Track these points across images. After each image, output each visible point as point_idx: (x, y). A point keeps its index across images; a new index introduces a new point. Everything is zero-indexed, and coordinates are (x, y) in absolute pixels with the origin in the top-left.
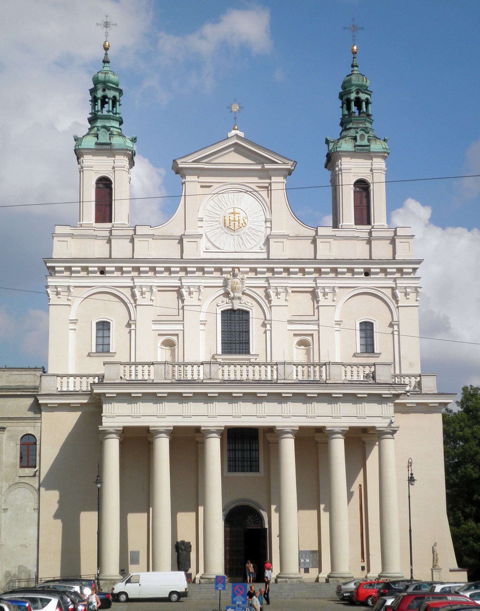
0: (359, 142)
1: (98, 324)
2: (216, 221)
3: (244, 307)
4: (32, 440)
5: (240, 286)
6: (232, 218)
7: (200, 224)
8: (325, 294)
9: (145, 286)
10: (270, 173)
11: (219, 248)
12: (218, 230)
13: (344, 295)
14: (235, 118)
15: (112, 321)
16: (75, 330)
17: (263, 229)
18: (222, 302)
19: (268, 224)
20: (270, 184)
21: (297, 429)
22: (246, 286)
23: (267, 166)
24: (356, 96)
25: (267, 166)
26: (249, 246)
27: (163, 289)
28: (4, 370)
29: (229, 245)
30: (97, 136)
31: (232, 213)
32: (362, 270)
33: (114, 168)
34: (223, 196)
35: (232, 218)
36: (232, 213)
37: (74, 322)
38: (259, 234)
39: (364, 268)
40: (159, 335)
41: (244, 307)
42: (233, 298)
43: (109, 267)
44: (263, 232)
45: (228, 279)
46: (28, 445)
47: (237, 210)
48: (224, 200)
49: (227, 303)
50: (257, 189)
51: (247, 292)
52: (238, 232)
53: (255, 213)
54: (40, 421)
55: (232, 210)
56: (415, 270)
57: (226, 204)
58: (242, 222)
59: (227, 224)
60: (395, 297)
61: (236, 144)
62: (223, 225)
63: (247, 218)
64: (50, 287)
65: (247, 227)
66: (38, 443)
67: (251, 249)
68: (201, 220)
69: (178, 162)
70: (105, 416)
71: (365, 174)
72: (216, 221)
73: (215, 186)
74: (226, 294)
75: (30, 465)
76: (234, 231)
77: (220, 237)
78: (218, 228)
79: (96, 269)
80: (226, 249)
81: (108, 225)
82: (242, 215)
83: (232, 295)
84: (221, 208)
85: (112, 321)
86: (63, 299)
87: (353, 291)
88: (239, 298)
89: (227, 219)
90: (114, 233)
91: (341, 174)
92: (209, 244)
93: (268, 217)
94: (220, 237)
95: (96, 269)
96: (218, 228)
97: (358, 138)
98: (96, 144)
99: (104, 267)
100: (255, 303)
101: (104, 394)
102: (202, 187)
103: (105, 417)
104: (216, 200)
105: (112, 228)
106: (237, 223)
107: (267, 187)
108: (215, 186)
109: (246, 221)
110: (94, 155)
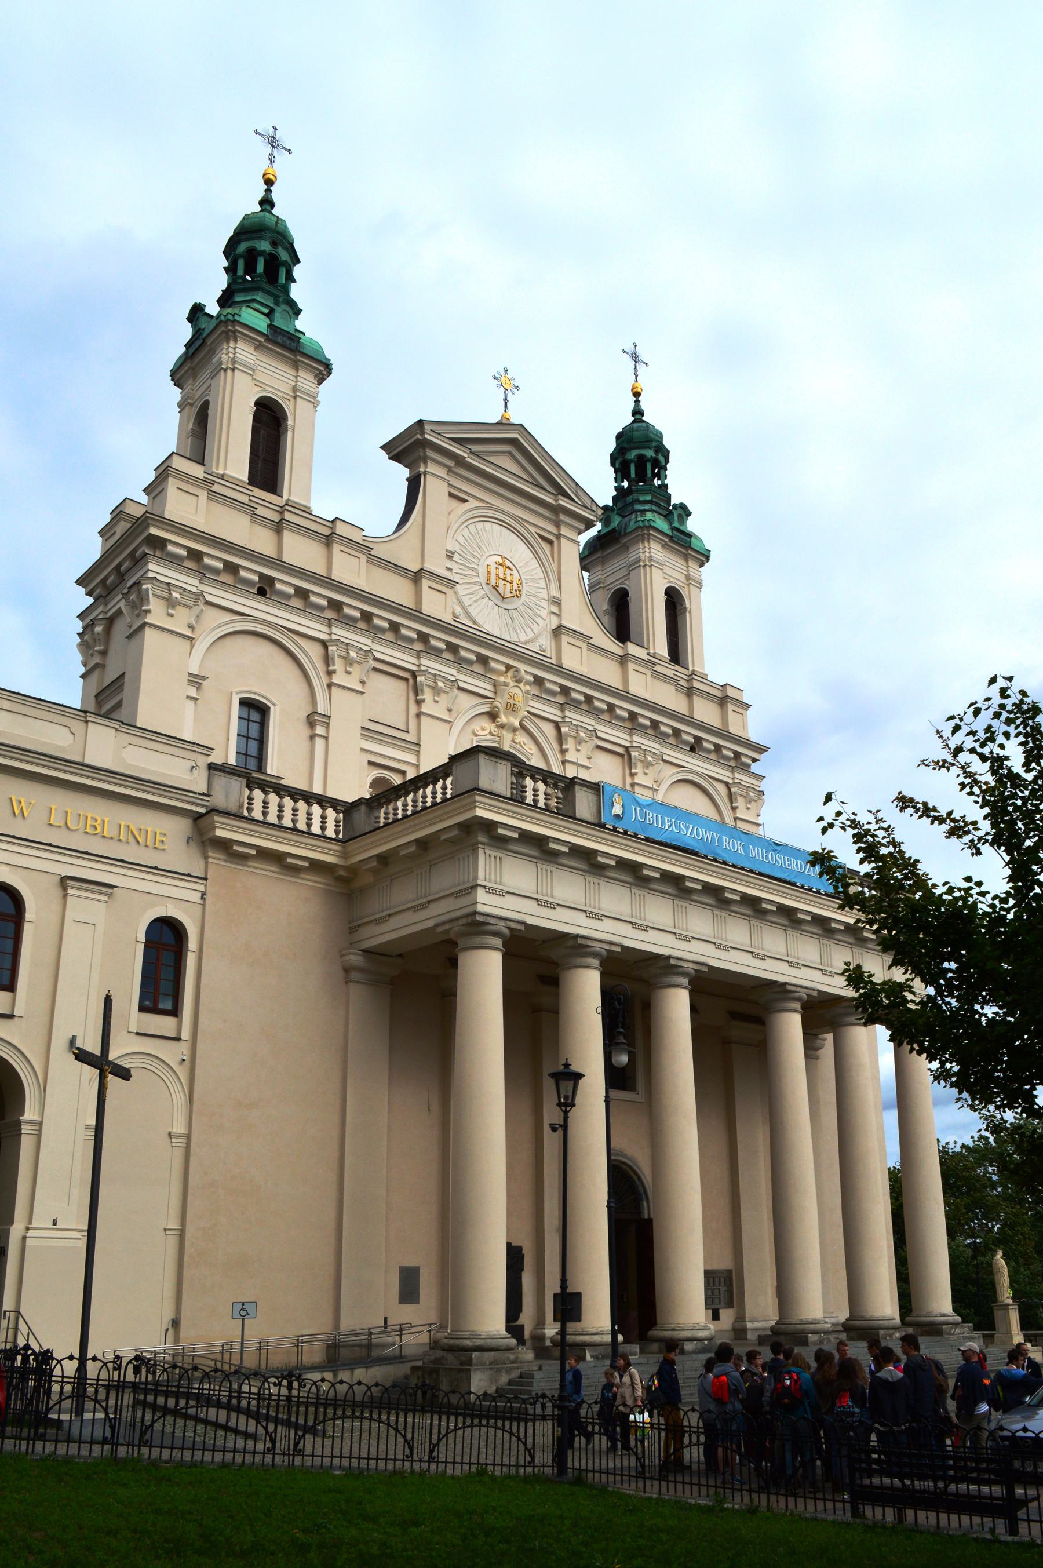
2: (472, 569)
3: (518, 751)
6: (502, 576)
7: (449, 564)
8: (647, 765)
9: (355, 646)
10: (562, 517)
11: (474, 622)
15: (274, 705)
16: (195, 699)
17: (544, 613)
18: (483, 729)
19: (555, 609)
20: (559, 536)
23: (563, 502)
24: (654, 455)
25: (563, 502)
26: (523, 638)
27: (384, 669)
32: (692, 740)
34: (484, 528)
37: (196, 680)
38: (539, 620)
40: (370, 763)
41: (518, 751)
42: (502, 726)
43: (285, 583)
47: (508, 564)
52: (507, 603)
55: (499, 559)
56: (754, 760)
59: (493, 582)
61: (513, 442)
62: (484, 581)
67: (526, 643)
69: (426, 427)
70: (484, 887)
71: (677, 580)
72: (472, 569)
74: (493, 716)
76: (503, 597)
77: (476, 601)
78: (475, 583)
83: (503, 719)
85: (274, 705)
86: (180, 621)
87: (678, 772)
92: (458, 610)
93: (555, 592)
94: (476, 601)
95: (256, 578)
96: (475, 583)
101: (489, 826)
102: (451, 495)
103: (483, 890)
104: (472, 528)
105: (287, 507)
108: (473, 503)
110: (259, 347)
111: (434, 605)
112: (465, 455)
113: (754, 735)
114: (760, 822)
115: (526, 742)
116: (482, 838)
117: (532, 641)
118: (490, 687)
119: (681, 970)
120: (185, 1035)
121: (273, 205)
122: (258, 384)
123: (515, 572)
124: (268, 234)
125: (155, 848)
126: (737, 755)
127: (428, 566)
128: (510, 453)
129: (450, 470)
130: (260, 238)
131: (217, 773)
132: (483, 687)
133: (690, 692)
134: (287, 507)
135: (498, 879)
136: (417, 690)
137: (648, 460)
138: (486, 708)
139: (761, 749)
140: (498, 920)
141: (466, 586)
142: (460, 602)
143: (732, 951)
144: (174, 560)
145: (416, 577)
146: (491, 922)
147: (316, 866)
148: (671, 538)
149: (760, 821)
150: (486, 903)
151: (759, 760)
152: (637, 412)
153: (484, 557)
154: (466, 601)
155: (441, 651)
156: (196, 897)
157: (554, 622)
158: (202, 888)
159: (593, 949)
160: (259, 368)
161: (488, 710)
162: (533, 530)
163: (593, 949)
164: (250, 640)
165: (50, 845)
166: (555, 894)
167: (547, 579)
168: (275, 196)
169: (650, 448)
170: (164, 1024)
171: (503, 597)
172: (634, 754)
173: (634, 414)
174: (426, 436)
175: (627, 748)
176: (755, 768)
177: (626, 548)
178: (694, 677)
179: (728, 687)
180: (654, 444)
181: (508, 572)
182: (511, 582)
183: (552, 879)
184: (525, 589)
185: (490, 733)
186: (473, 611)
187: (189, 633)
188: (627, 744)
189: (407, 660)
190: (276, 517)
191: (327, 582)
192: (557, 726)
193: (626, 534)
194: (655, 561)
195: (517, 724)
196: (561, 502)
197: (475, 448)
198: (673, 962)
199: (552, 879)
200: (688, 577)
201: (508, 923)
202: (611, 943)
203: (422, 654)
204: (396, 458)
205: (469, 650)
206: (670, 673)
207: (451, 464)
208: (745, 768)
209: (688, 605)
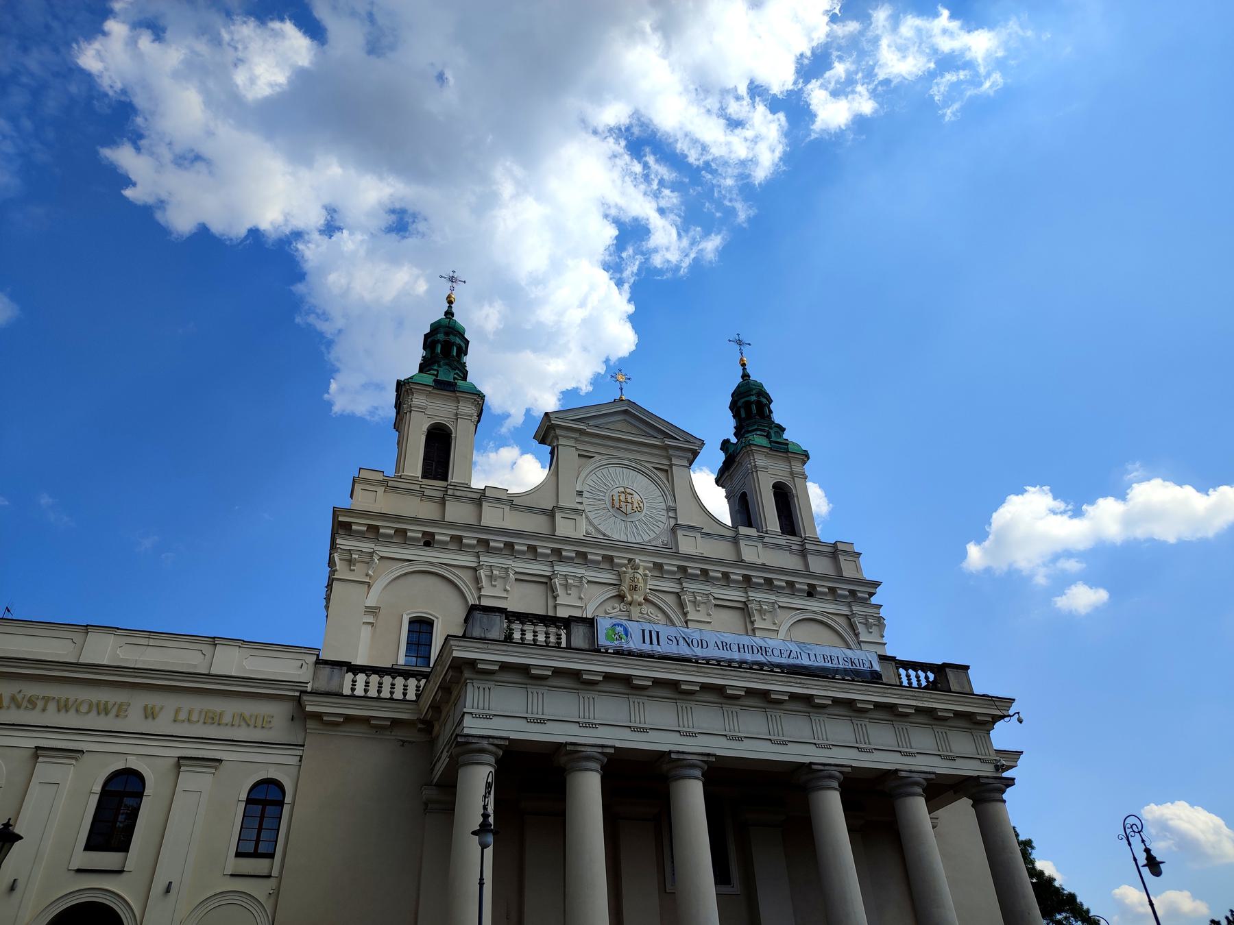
0: (774, 439)
1: (412, 622)
4: (273, 795)
5: (642, 585)
6: (623, 500)
7: (579, 500)
10: (671, 452)
11: (604, 535)
12: (605, 511)
13: (787, 619)
14: (621, 389)
15: (437, 618)
16: (372, 624)
17: (664, 519)
19: (671, 514)
20: (671, 466)
21: (849, 770)
22: (650, 589)
23: (669, 442)
25: (669, 442)
26: (646, 538)
28: (240, 645)
29: (618, 533)
30: (437, 376)
31: (623, 493)
33: (456, 414)
35: (623, 497)
36: (623, 493)
37: (373, 611)
39: (809, 585)
43: (442, 535)
44: (665, 523)
45: (625, 573)
46: (265, 803)
47: (628, 490)
48: (609, 476)
49: (620, 610)
50: (652, 469)
51: (650, 597)
53: (653, 499)
54: (301, 752)
55: (622, 490)
56: (871, 595)
57: (613, 480)
58: (636, 505)
60: (853, 627)
61: (626, 412)
62: (608, 505)
63: (642, 502)
64: (339, 550)
65: (643, 514)
66: (288, 799)
67: (650, 542)
68: (580, 493)
70: (471, 713)
71: (784, 477)
73: (597, 457)
74: (621, 597)
75: (279, 816)
76: (627, 514)
78: (603, 509)
79: (420, 535)
80: (616, 537)
81: (442, 484)
82: (636, 496)
83: (629, 598)
84: (606, 485)
85: (437, 618)
86: (358, 573)
88: (640, 604)
89: (616, 498)
90: (450, 492)
91: (756, 472)
92: (591, 529)
93: (670, 503)
96: (603, 509)
97: (773, 435)
98: (435, 381)
99: (433, 534)
100: (660, 616)
101: (472, 663)
103: (470, 716)
104: (599, 474)
105: (448, 487)
106: (629, 506)
107: (667, 471)
109: (641, 505)
110: (429, 394)
111: (564, 528)
112: (585, 428)
113: (869, 575)
114: (884, 642)
115: (653, 612)
116: (467, 674)
117: (654, 539)
118: (614, 577)
119: (685, 762)
120: (275, 873)
121: (453, 315)
122: (430, 416)
123: (636, 496)
124: (442, 330)
125: (263, 727)
126: (853, 593)
127: (561, 504)
128: (625, 420)
129: (576, 440)
130: (437, 333)
131: (321, 666)
132: (609, 577)
133: (803, 553)
134: (448, 487)
135: (824, 737)
136: (553, 589)
137: (752, 403)
138: (614, 593)
139: (877, 584)
140: (481, 739)
141: (596, 512)
142: (591, 523)
143: (700, 736)
144: (359, 535)
145: (551, 514)
146: (473, 741)
147: (395, 722)
148: (771, 449)
149: (884, 640)
150: (472, 726)
151: (875, 593)
152: (745, 376)
153: (609, 491)
154: (596, 522)
155: (572, 558)
156: (295, 761)
157: (672, 522)
158: (300, 753)
159: (581, 754)
160: (429, 407)
161: (617, 593)
162: (649, 465)
163: (581, 754)
164: (414, 576)
165: (47, 727)
166: (953, 749)
167: (664, 495)
168: (454, 310)
169: (753, 395)
170: (260, 865)
171: (627, 514)
172: (752, 606)
173: (743, 377)
174: (553, 422)
175: (744, 603)
176: (874, 600)
177: (740, 463)
178: (806, 541)
179: (838, 544)
180: (754, 392)
181: (630, 496)
182: (632, 503)
183: (908, 733)
184: (645, 506)
185: (620, 610)
186: (601, 528)
187: (367, 580)
188: (743, 600)
189: (542, 569)
190: (440, 494)
191: (478, 528)
192: (678, 595)
193: (737, 454)
194: (761, 468)
195: (641, 599)
196: (666, 442)
197: (591, 423)
198: (673, 756)
199: (908, 733)
200: (792, 473)
201: (491, 740)
202: (603, 746)
203: (554, 563)
204: (542, 441)
205: (595, 555)
206: (784, 542)
207: (577, 435)
208: (865, 602)
209: (794, 492)
